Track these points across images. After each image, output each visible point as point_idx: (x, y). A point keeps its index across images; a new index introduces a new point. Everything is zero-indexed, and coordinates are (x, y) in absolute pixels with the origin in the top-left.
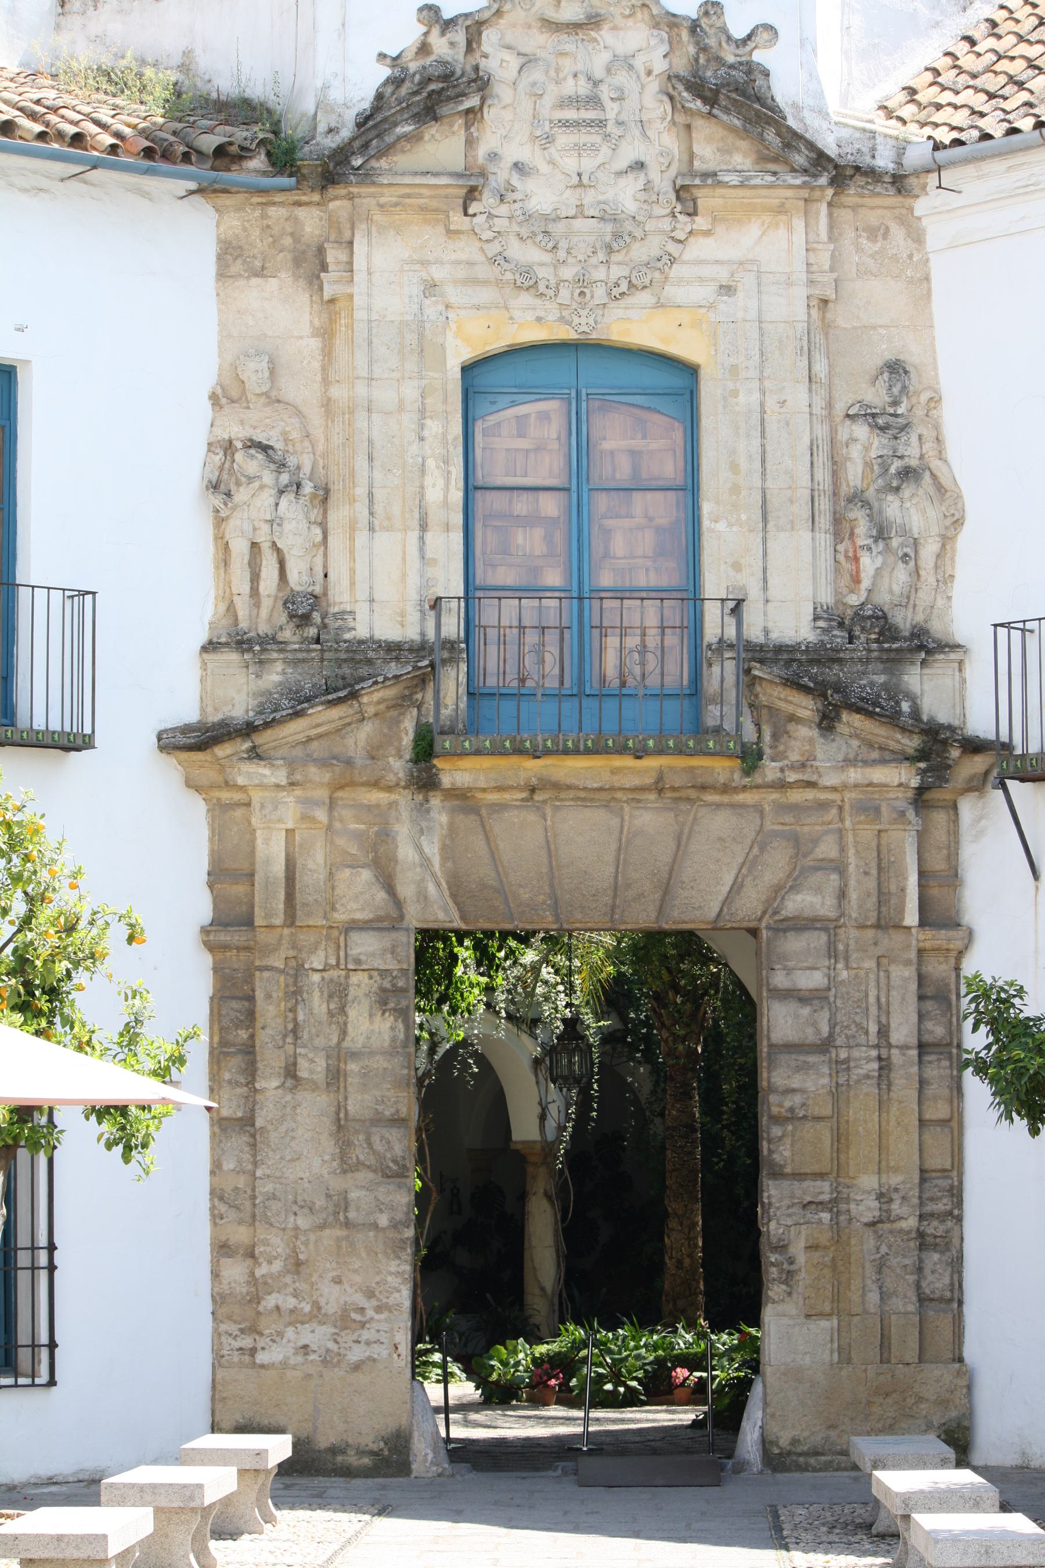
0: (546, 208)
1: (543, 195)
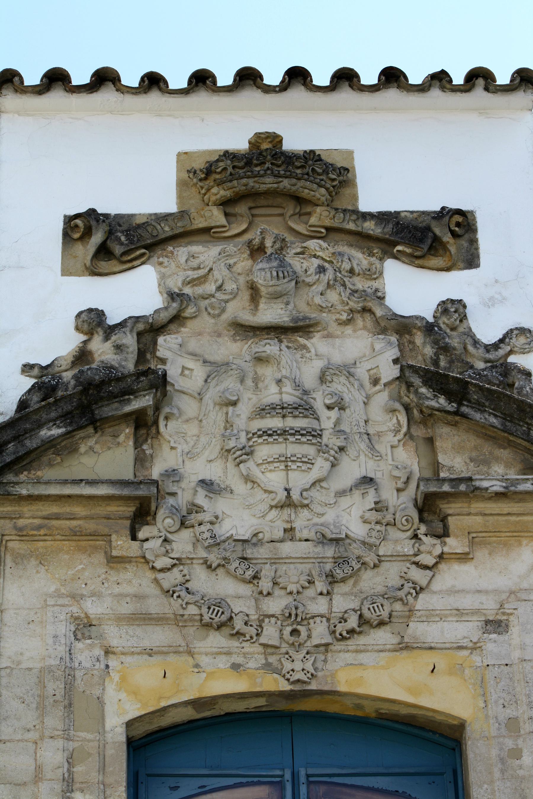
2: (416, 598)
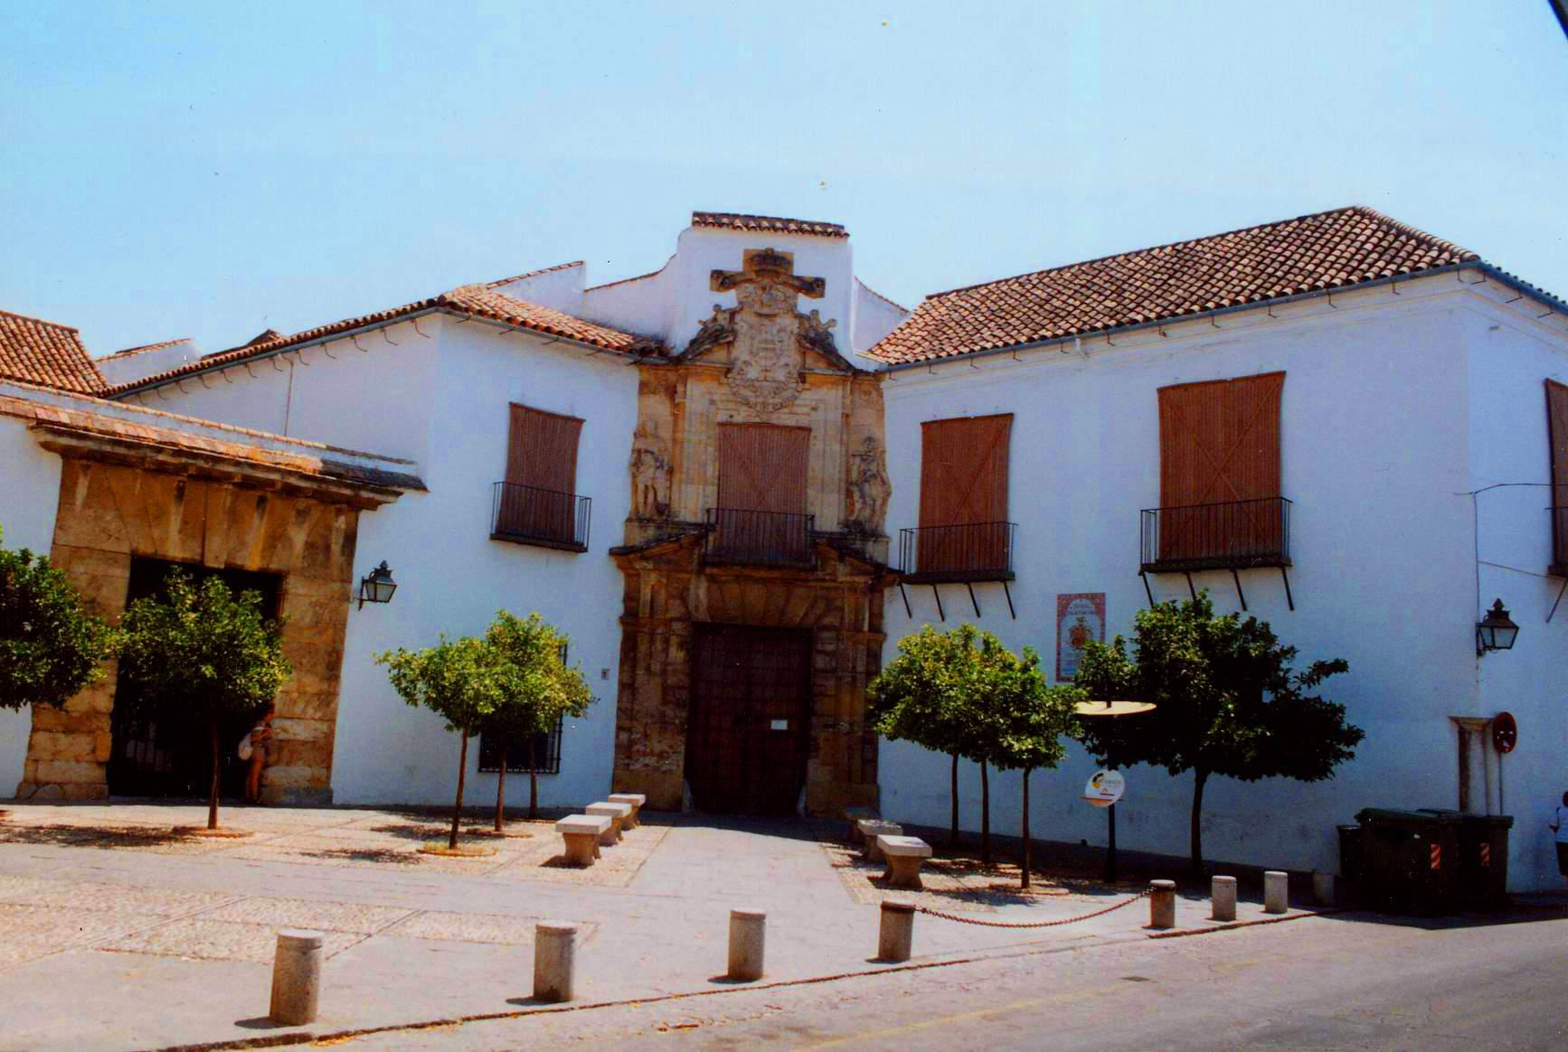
1: (753, 373)
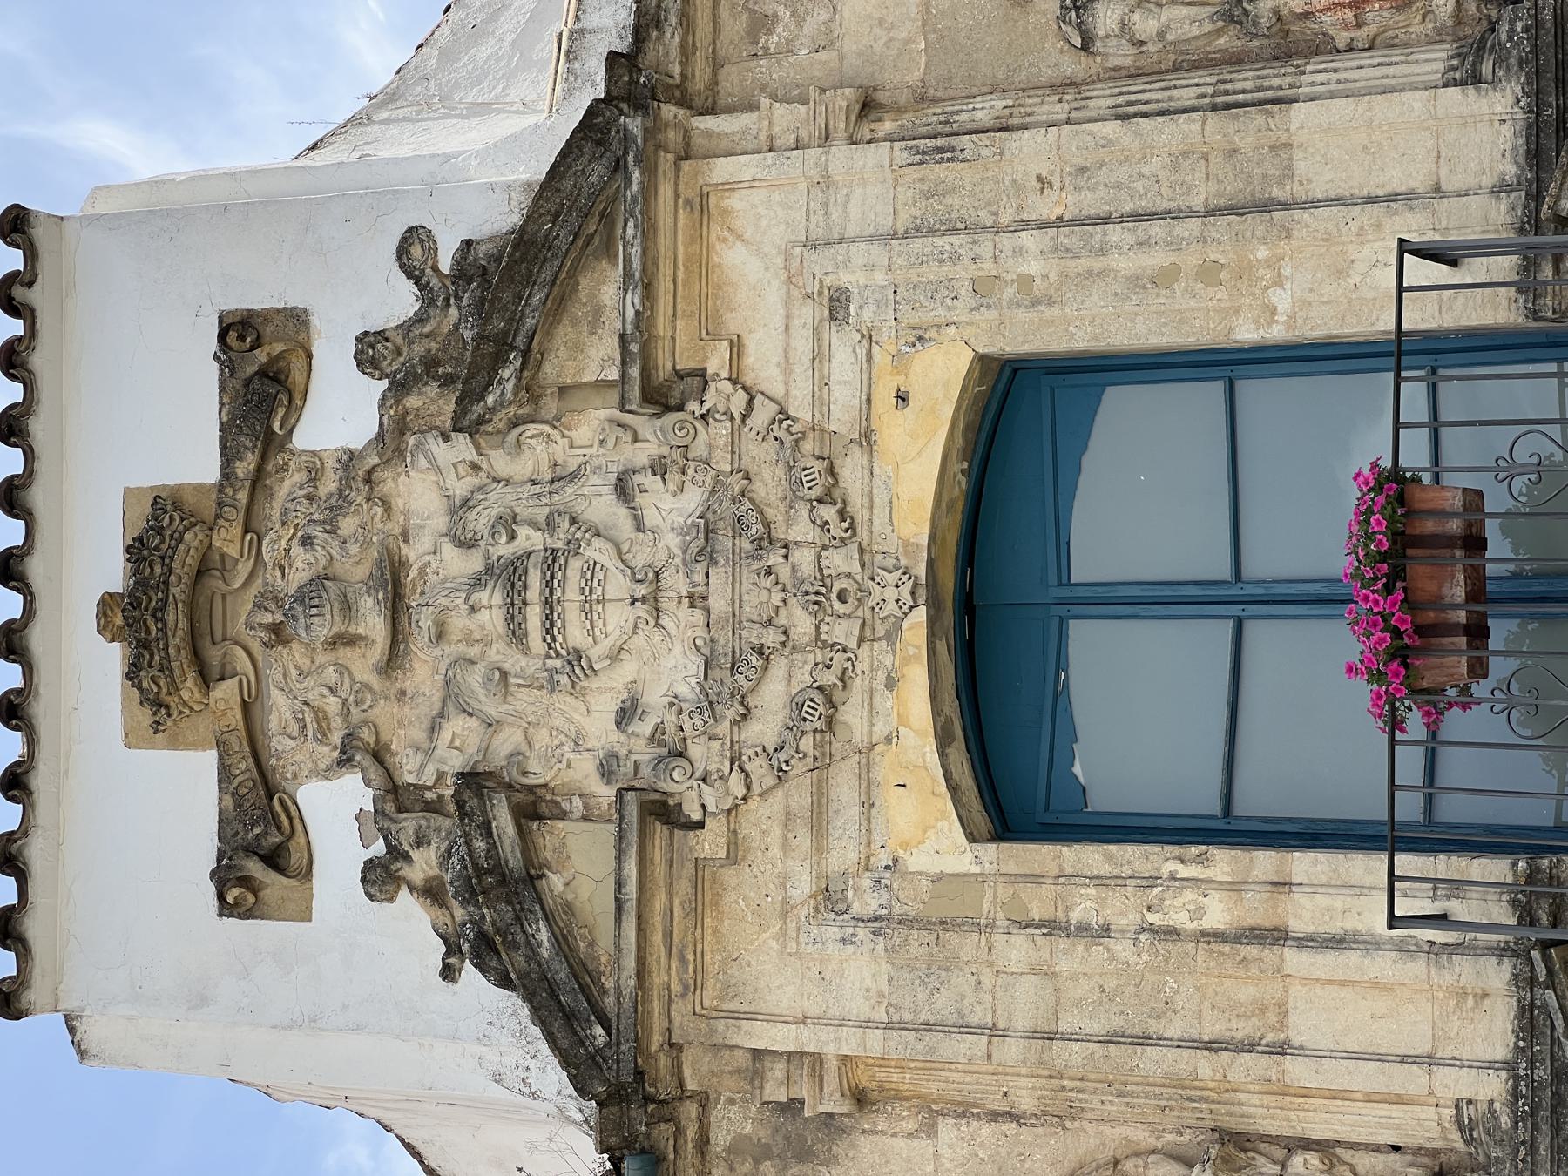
0: (695, 665)
2: (795, 420)
